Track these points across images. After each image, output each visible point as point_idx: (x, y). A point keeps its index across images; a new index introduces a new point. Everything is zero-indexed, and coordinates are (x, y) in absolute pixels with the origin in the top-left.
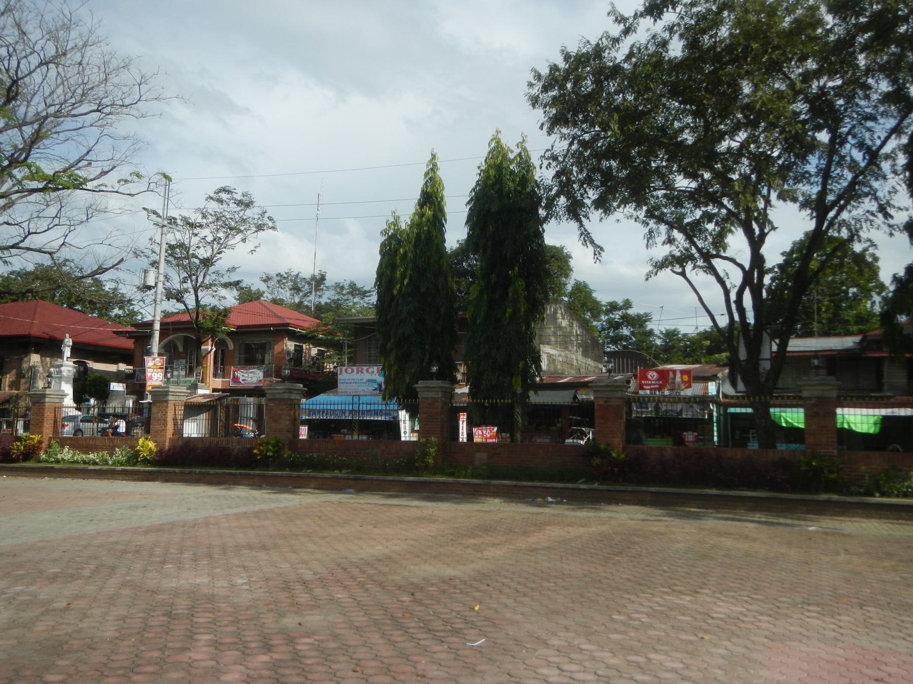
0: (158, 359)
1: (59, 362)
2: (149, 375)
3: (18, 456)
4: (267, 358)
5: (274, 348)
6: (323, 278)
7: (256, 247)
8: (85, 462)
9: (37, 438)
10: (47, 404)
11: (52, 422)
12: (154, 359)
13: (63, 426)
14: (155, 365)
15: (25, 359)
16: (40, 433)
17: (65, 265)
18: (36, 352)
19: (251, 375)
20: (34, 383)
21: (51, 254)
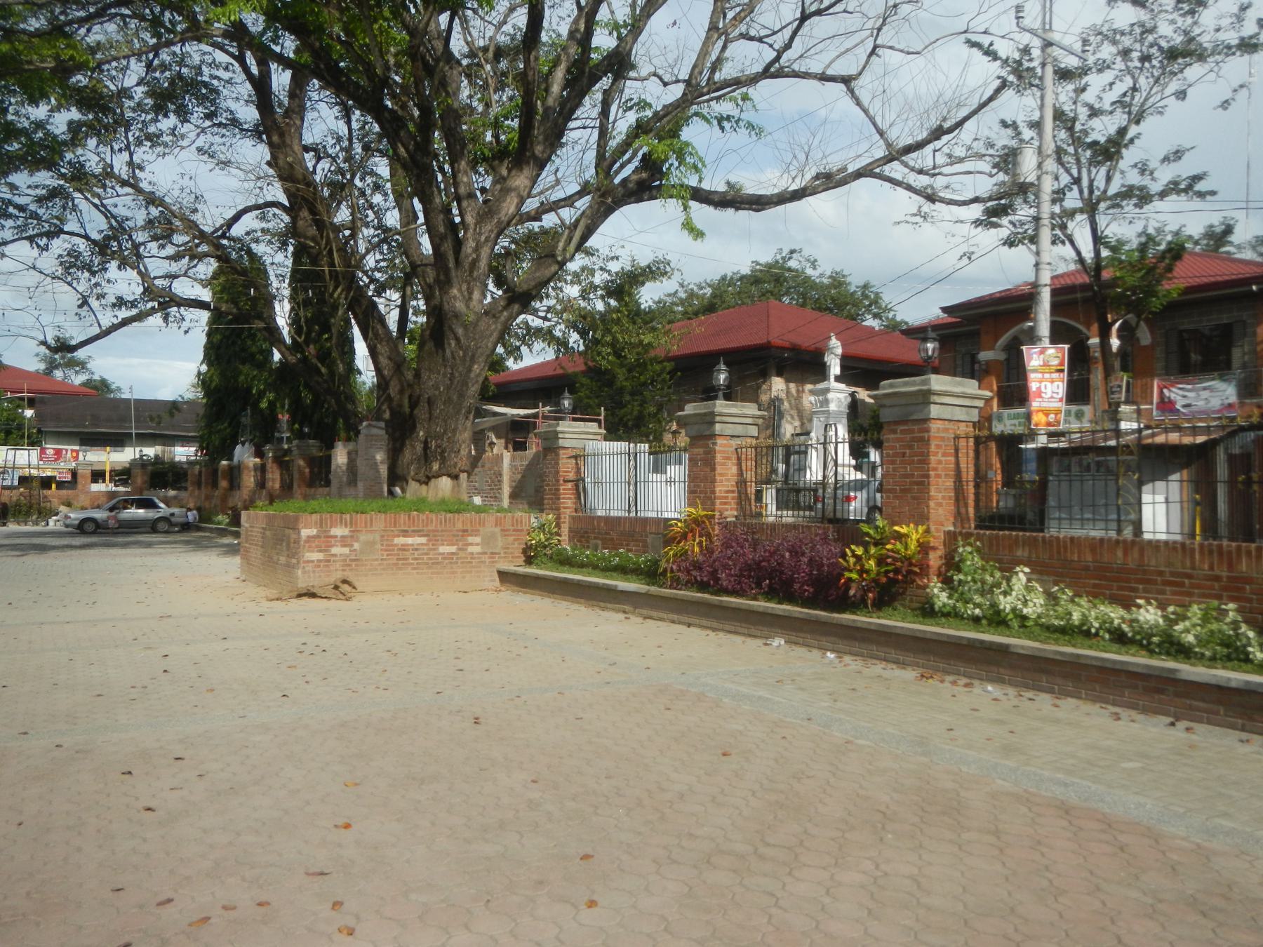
0: (1051, 351)
1: (821, 386)
2: (1033, 386)
3: (865, 591)
4: (1237, 354)
5: (1255, 334)
6: (1228, 230)
7: (1235, 91)
8: (1119, 638)
9: (913, 533)
10: (934, 426)
11: (950, 483)
12: (1042, 352)
13: (848, 499)
14: (1046, 364)
15: (764, 387)
16: (921, 518)
17: (790, 258)
18: (779, 374)
19: (1205, 394)
20: (779, 426)
21: (846, 80)
